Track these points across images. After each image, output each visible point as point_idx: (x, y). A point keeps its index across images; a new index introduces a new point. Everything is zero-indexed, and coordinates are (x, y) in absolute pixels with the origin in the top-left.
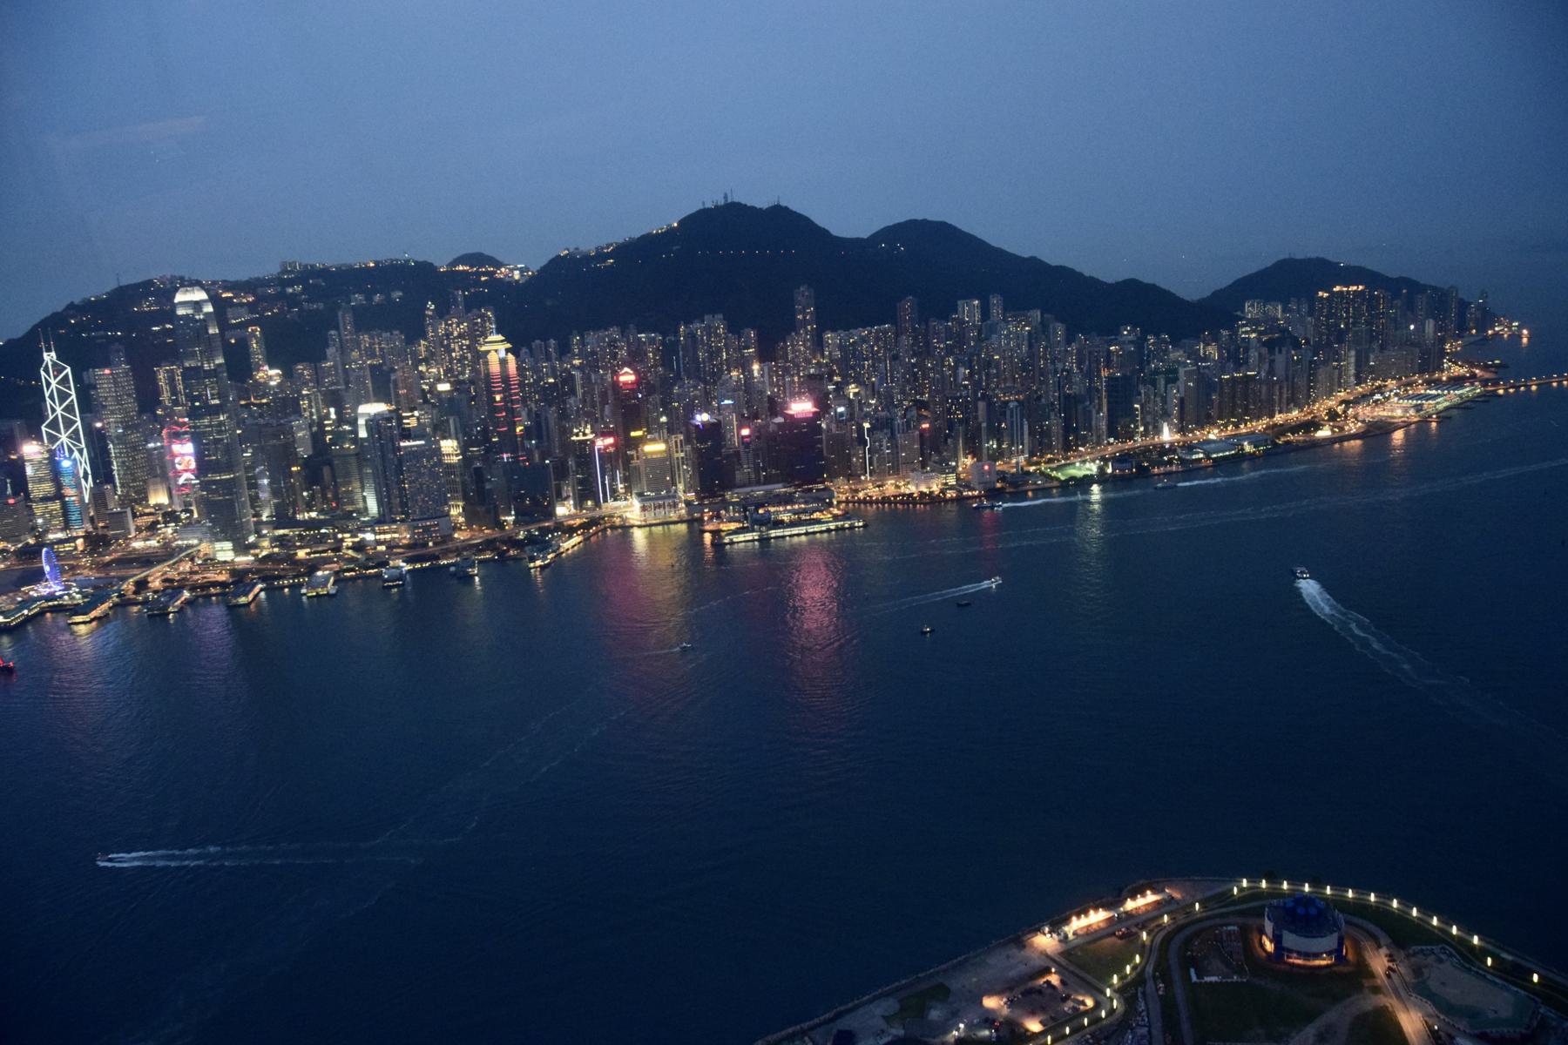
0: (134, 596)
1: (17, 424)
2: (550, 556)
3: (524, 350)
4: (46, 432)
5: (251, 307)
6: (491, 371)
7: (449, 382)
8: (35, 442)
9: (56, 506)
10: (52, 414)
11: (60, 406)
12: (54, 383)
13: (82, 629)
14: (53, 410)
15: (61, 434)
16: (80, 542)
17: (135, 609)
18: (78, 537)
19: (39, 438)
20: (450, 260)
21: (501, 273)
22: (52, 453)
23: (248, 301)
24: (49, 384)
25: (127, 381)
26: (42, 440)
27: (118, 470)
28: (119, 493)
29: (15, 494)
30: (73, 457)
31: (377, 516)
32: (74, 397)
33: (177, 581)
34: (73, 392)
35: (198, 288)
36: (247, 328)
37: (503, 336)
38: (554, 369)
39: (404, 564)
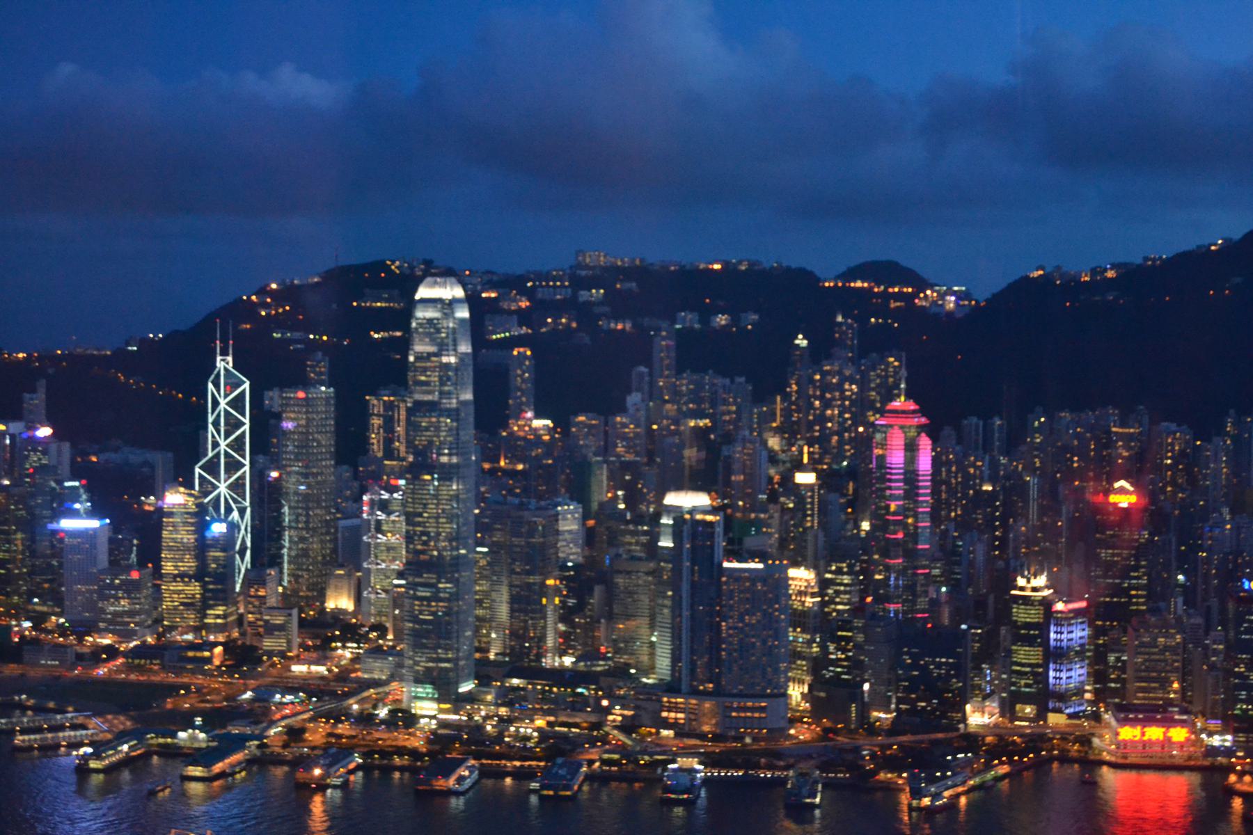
0: (280, 750)
1: (161, 460)
2: (946, 794)
3: (948, 431)
4: (201, 476)
5: (523, 317)
6: (888, 460)
7: (814, 470)
8: (182, 489)
9: (195, 589)
10: (213, 450)
11: (226, 437)
12: (223, 403)
13: (196, 788)
14: (216, 445)
15: (219, 482)
16: (219, 650)
17: (280, 772)
18: (216, 644)
19: (189, 485)
20: (842, 268)
21: (926, 296)
22: (202, 510)
23: (520, 310)
24: (216, 403)
25: (326, 411)
26: (192, 488)
27: (290, 549)
28: (285, 583)
29: (141, 564)
30: (230, 518)
31: (669, 678)
32: (247, 427)
33: (347, 737)
34: (247, 421)
35: (453, 279)
36: (513, 350)
37: (916, 402)
38: (994, 465)
39: (701, 767)
